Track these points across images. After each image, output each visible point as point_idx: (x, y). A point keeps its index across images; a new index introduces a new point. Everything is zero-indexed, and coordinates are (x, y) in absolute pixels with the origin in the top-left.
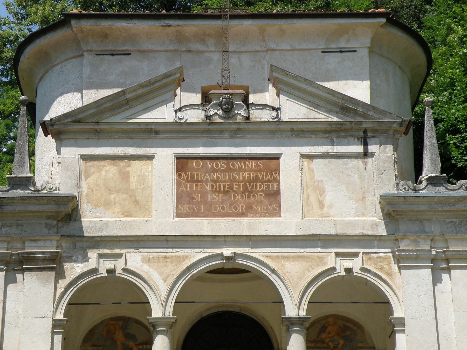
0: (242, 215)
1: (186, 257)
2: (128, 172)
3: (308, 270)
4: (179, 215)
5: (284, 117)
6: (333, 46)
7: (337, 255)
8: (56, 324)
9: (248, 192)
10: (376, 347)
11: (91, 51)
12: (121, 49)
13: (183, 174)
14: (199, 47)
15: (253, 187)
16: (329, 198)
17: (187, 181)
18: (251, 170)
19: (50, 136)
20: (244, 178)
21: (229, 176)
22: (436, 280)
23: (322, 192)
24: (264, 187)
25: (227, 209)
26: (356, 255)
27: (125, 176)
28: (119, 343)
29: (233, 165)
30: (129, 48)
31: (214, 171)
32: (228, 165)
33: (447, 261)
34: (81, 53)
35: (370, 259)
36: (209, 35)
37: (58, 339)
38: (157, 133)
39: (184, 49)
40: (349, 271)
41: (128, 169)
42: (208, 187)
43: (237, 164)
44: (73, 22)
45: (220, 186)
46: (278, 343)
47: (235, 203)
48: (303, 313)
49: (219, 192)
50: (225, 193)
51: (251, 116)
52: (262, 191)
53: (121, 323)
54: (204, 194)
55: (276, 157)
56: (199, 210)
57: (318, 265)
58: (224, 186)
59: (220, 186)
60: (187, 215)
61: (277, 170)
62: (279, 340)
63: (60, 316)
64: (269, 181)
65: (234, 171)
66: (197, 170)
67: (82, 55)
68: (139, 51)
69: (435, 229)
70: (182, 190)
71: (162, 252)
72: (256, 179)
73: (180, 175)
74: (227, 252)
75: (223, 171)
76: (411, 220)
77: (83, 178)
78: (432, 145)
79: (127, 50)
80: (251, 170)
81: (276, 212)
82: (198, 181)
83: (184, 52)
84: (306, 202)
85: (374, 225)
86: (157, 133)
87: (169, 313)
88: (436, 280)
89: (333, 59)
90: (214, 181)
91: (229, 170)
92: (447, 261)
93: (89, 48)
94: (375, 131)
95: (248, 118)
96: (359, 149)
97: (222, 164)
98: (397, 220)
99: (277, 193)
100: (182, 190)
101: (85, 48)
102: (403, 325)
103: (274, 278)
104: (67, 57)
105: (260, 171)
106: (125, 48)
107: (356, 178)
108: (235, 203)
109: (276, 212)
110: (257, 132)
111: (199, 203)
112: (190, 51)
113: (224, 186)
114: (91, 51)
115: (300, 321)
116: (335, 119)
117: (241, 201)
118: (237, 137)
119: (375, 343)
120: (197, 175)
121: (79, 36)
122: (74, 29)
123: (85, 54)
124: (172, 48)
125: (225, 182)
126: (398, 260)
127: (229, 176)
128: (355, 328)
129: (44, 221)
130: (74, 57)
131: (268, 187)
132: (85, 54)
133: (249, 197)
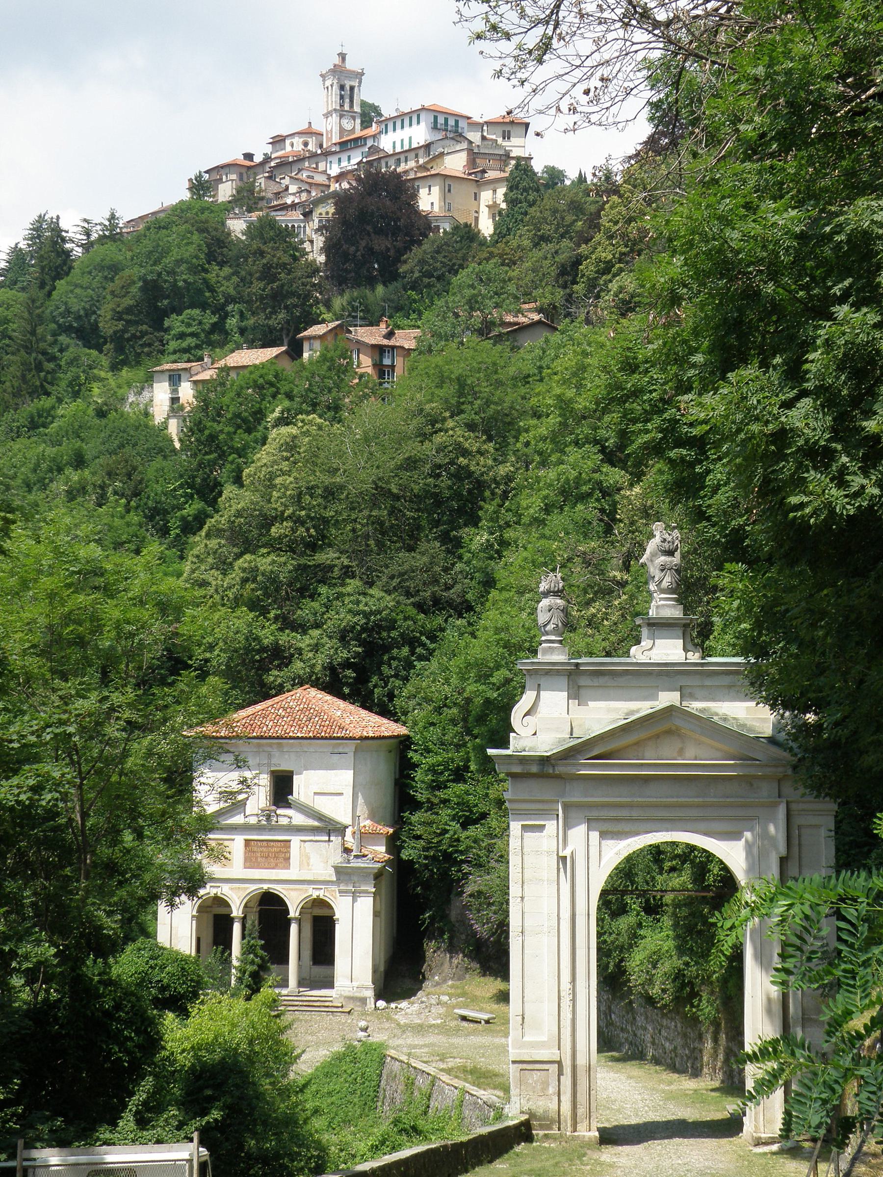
5: (295, 822)
6: (336, 751)
8: (193, 916)
9: (276, 857)
14: (269, 749)
16: (312, 861)
22: (354, 901)
23: (309, 858)
54: (256, 858)
63: (195, 913)
69: (355, 879)
71: (237, 885)
74: (265, 886)
81: (288, 868)
84: (301, 864)
85: (330, 875)
88: (354, 901)
89: (336, 757)
96: (327, 838)
97: (265, 844)
107: (324, 852)
109: (288, 868)
115: (295, 919)
116: (316, 824)
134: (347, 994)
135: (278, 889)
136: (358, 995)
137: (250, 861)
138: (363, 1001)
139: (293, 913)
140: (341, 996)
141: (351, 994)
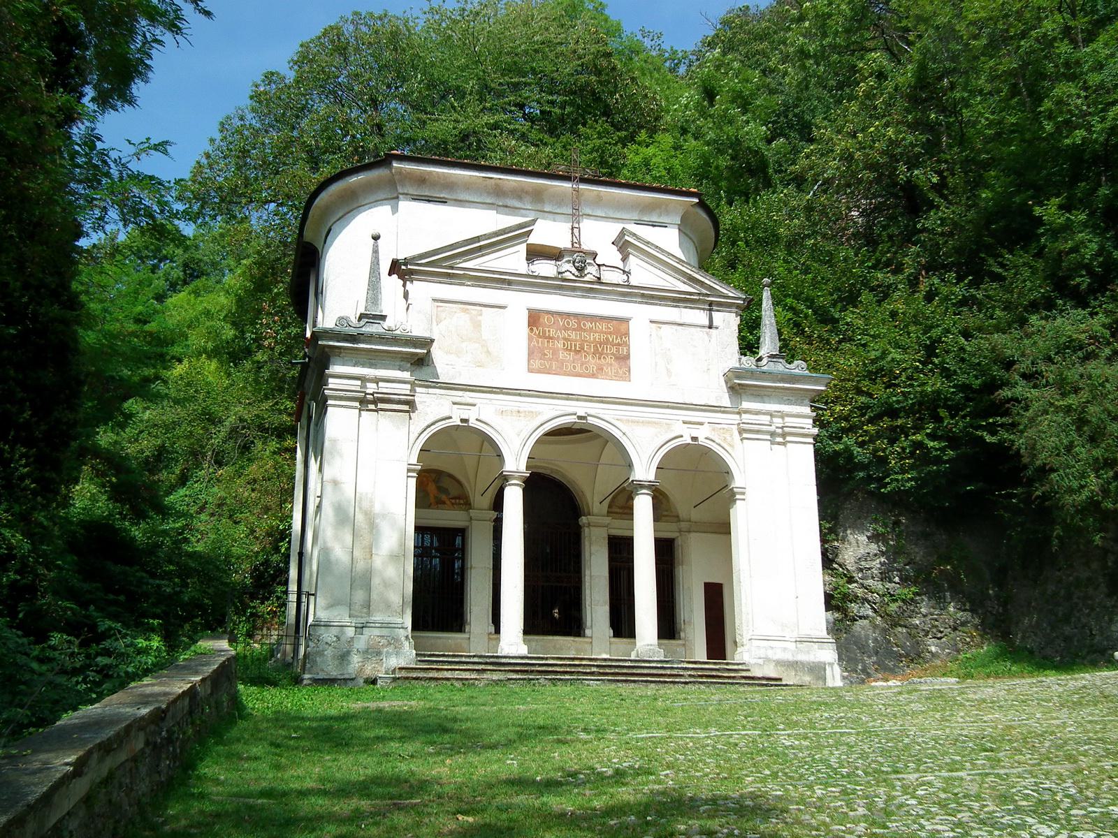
0: (593, 376)
1: (539, 413)
2: (480, 321)
3: (656, 435)
4: (530, 371)
5: (633, 282)
7: (684, 422)
9: (598, 354)
10: (681, 516)
11: (407, 194)
12: (438, 196)
13: (535, 329)
15: (603, 349)
17: (539, 336)
18: (602, 332)
19: (395, 276)
20: (595, 339)
21: (580, 335)
24: (614, 350)
25: (578, 369)
26: (701, 424)
27: (477, 325)
28: (432, 495)
29: (584, 325)
30: (446, 196)
31: (566, 329)
32: (579, 324)
33: (784, 435)
34: (395, 195)
35: (714, 430)
36: (527, 193)
37: (413, 482)
38: (509, 283)
39: (501, 204)
40: (695, 439)
41: (479, 318)
42: (560, 345)
43: (588, 325)
44: (395, 164)
45: (571, 344)
46: (588, 507)
47: (586, 363)
48: (652, 478)
49: (570, 350)
50: (577, 352)
51: (602, 278)
52: (612, 354)
53: (434, 475)
54: (555, 352)
55: (626, 321)
56: (551, 366)
57: (666, 432)
58: (576, 345)
59: (571, 344)
60: (539, 371)
61: (627, 334)
62: (590, 505)
63: (414, 460)
64: (619, 344)
65: (585, 331)
66: (549, 327)
67: (397, 198)
68: (455, 200)
70: (534, 345)
72: (607, 342)
73: (531, 330)
75: (574, 330)
76: (753, 395)
77: (435, 323)
78: (771, 324)
79: (444, 198)
80: (602, 332)
81: (626, 375)
82: (550, 338)
83: (500, 206)
86: (509, 283)
87: (523, 467)
90: (565, 339)
91: (580, 329)
92: (784, 435)
93: (406, 192)
94: (720, 304)
95: (599, 278)
97: (573, 323)
98: (740, 394)
99: (627, 357)
100: (534, 345)
101: (400, 191)
102: (743, 494)
103: (624, 440)
104: (379, 198)
105: (610, 333)
106: (442, 196)
108: (586, 363)
109: (626, 375)
110: (608, 292)
111: (550, 359)
112: (506, 206)
113: (576, 345)
114: (407, 194)
117: (592, 362)
118: (589, 297)
119: (680, 513)
120: (549, 331)
121: (397, 177)
122: (393, 171)
123: (401, 196)
124: (488, 201)
125: (576, 341)
126: (741, 431)
127: (580, 335)
128: (661, 497)
129: (398, 363)
130: (386, 199)
131: (618, 350)
132: (401, 196)
133: (600, 358)
134: (780, 656)
135: (604, 417)
136: (802, 657)
137: (539, 358)
138: (818, 670)
139: (644, 471)
140: (767, 660)
141: (791, 658)
